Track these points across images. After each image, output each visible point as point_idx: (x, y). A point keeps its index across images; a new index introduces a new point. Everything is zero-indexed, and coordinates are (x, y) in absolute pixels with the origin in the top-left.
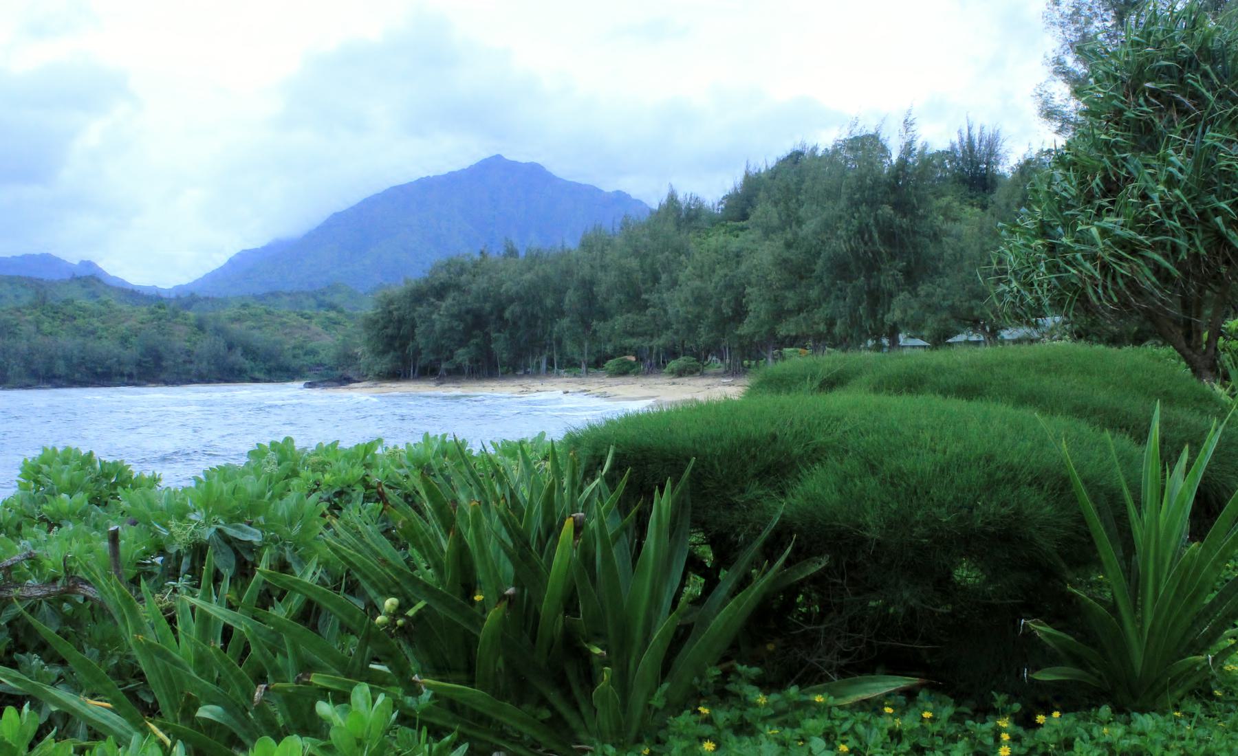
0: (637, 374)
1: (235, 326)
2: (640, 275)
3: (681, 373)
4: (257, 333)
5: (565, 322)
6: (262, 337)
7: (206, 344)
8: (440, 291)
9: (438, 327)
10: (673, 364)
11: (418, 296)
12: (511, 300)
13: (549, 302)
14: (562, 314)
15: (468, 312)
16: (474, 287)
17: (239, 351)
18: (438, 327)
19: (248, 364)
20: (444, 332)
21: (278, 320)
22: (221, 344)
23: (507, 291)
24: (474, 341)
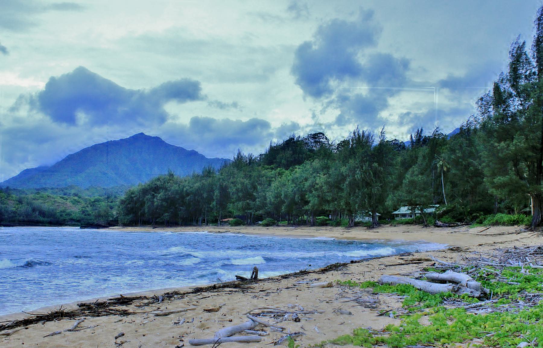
0: (244, 225)
1: (34, 201)
2: (249, 186)
3: (267, 225)
4: (43, 205)
5: (214, 203)
6: (46, 206)
7: (23, 208)
8: (154, 189)
9: (156, 204)
10: (264, 222)
11: (145, 191)
12: (188, 195)
13: (205, 195)
14: (213, 200)
15: (168, 199)
16: (173, 188)
17: (37, 213)
18: (156, 204)
19: (41, 219)
20: (158, 206)
21: (53, 200)
22: (30, 209)
23: (186, 191)
24: (172, 210)
